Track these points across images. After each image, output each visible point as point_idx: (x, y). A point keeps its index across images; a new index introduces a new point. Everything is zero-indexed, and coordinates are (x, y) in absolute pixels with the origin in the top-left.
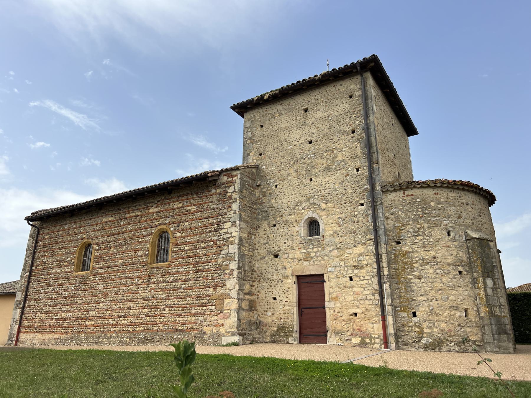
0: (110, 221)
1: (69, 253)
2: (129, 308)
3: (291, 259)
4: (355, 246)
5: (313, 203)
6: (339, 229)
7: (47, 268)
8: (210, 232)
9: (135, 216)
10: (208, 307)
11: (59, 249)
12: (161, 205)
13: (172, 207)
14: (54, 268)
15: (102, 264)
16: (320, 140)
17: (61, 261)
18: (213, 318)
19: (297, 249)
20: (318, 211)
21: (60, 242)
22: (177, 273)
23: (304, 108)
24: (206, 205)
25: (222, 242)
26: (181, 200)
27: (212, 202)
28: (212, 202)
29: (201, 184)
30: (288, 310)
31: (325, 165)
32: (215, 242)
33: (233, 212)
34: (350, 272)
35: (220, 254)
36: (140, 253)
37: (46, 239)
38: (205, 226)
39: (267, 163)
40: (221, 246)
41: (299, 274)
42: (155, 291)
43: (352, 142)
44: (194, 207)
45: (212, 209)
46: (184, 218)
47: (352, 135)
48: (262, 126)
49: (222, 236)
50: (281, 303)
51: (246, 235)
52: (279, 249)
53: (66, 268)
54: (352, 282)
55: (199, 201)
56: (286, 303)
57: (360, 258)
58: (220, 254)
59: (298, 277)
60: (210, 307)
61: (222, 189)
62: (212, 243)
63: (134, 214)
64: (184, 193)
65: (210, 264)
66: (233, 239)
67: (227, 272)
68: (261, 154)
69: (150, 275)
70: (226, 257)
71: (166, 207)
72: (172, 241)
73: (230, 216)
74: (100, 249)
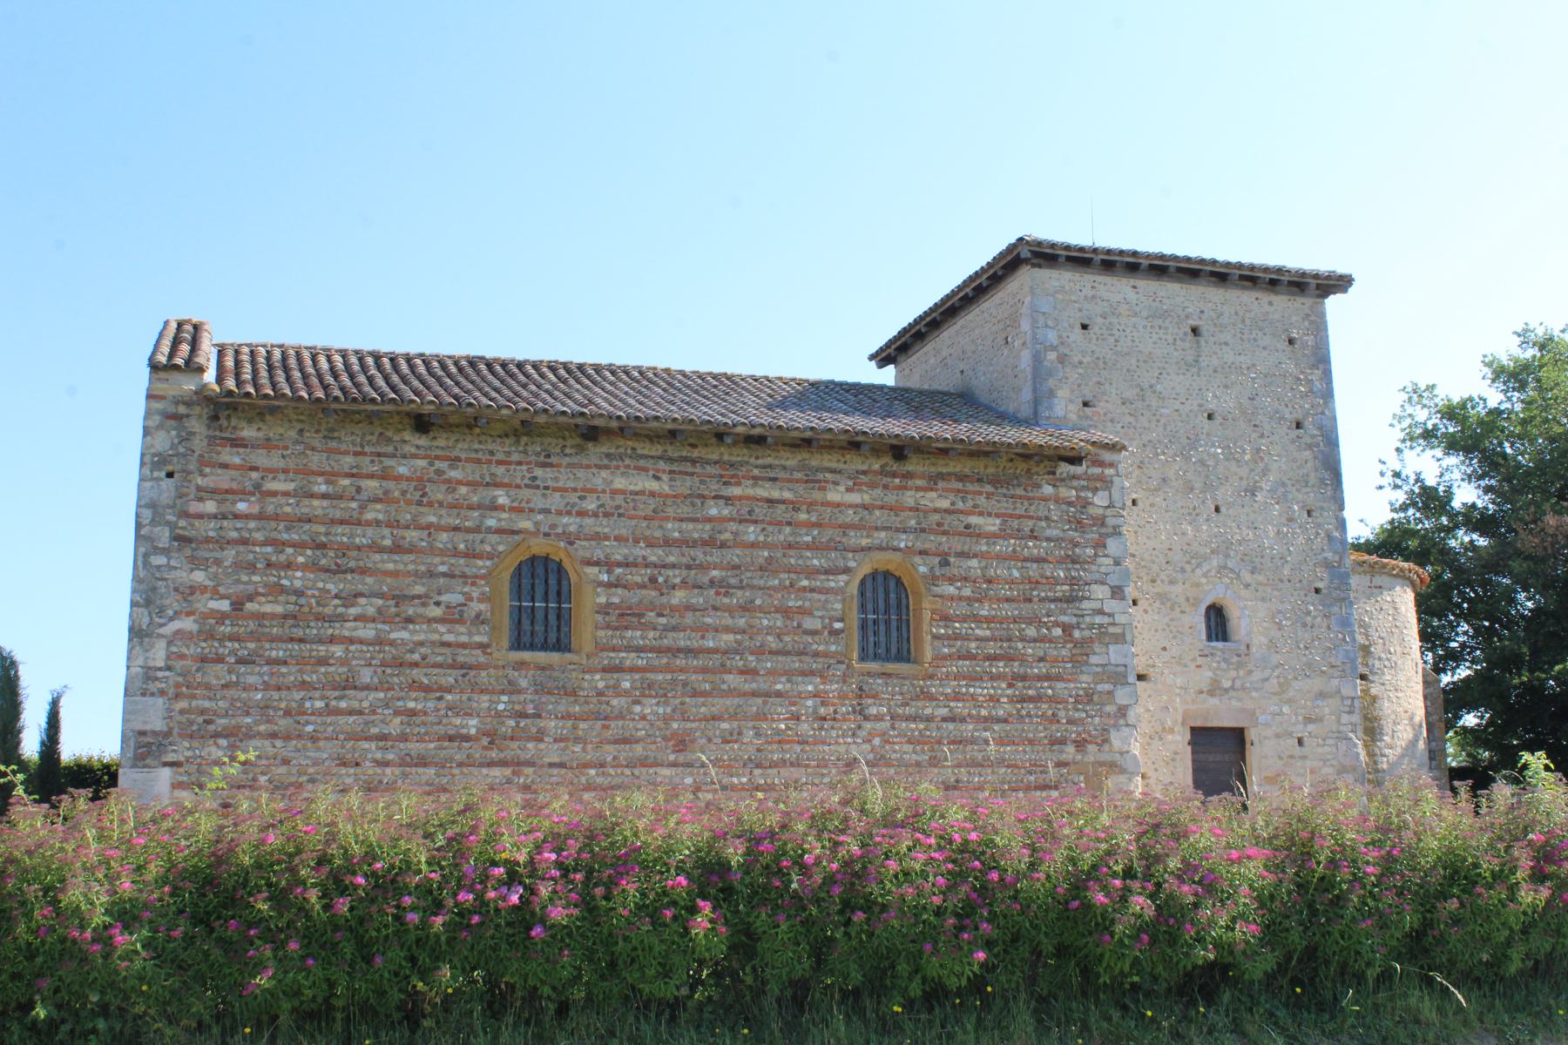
0: (652, 494)
1: (444, 575)
5: (1225, 567)
6: (1279, 634)
7: (320, 617)
9: (771, 502)
11: (376, 548)
12: (872, 486)
13: (911, 502)
17: (400, 599)
19: (1192, 666)
22: (957, 697)
24: (1031, 523)
28: (1047, 518)
31: (1244, 483)
32: (1067, 629)
34: (1301, 727)
36: (809, 623)
41: (1199, 724)
42: (887, 742)
43: (1299, 449)
44: (990, 520)
45: (1048, 539)
48: (1084, 327)
49: (1088, 619)
53: (442, 628)
55: (1005, 506)
57: (1319, 702)
58: (1086, 663)
59: (1193, 729)
62: (1058, 632)
63: (762, 491)
64: (951, 469)
65: (1060, 685)
66: (1118, 630)
67: (1108, 708)
68: (1086, 404)
70: (1104, 672)
71: (891, 498)
72: (927, 605)
73: (1103, 569)
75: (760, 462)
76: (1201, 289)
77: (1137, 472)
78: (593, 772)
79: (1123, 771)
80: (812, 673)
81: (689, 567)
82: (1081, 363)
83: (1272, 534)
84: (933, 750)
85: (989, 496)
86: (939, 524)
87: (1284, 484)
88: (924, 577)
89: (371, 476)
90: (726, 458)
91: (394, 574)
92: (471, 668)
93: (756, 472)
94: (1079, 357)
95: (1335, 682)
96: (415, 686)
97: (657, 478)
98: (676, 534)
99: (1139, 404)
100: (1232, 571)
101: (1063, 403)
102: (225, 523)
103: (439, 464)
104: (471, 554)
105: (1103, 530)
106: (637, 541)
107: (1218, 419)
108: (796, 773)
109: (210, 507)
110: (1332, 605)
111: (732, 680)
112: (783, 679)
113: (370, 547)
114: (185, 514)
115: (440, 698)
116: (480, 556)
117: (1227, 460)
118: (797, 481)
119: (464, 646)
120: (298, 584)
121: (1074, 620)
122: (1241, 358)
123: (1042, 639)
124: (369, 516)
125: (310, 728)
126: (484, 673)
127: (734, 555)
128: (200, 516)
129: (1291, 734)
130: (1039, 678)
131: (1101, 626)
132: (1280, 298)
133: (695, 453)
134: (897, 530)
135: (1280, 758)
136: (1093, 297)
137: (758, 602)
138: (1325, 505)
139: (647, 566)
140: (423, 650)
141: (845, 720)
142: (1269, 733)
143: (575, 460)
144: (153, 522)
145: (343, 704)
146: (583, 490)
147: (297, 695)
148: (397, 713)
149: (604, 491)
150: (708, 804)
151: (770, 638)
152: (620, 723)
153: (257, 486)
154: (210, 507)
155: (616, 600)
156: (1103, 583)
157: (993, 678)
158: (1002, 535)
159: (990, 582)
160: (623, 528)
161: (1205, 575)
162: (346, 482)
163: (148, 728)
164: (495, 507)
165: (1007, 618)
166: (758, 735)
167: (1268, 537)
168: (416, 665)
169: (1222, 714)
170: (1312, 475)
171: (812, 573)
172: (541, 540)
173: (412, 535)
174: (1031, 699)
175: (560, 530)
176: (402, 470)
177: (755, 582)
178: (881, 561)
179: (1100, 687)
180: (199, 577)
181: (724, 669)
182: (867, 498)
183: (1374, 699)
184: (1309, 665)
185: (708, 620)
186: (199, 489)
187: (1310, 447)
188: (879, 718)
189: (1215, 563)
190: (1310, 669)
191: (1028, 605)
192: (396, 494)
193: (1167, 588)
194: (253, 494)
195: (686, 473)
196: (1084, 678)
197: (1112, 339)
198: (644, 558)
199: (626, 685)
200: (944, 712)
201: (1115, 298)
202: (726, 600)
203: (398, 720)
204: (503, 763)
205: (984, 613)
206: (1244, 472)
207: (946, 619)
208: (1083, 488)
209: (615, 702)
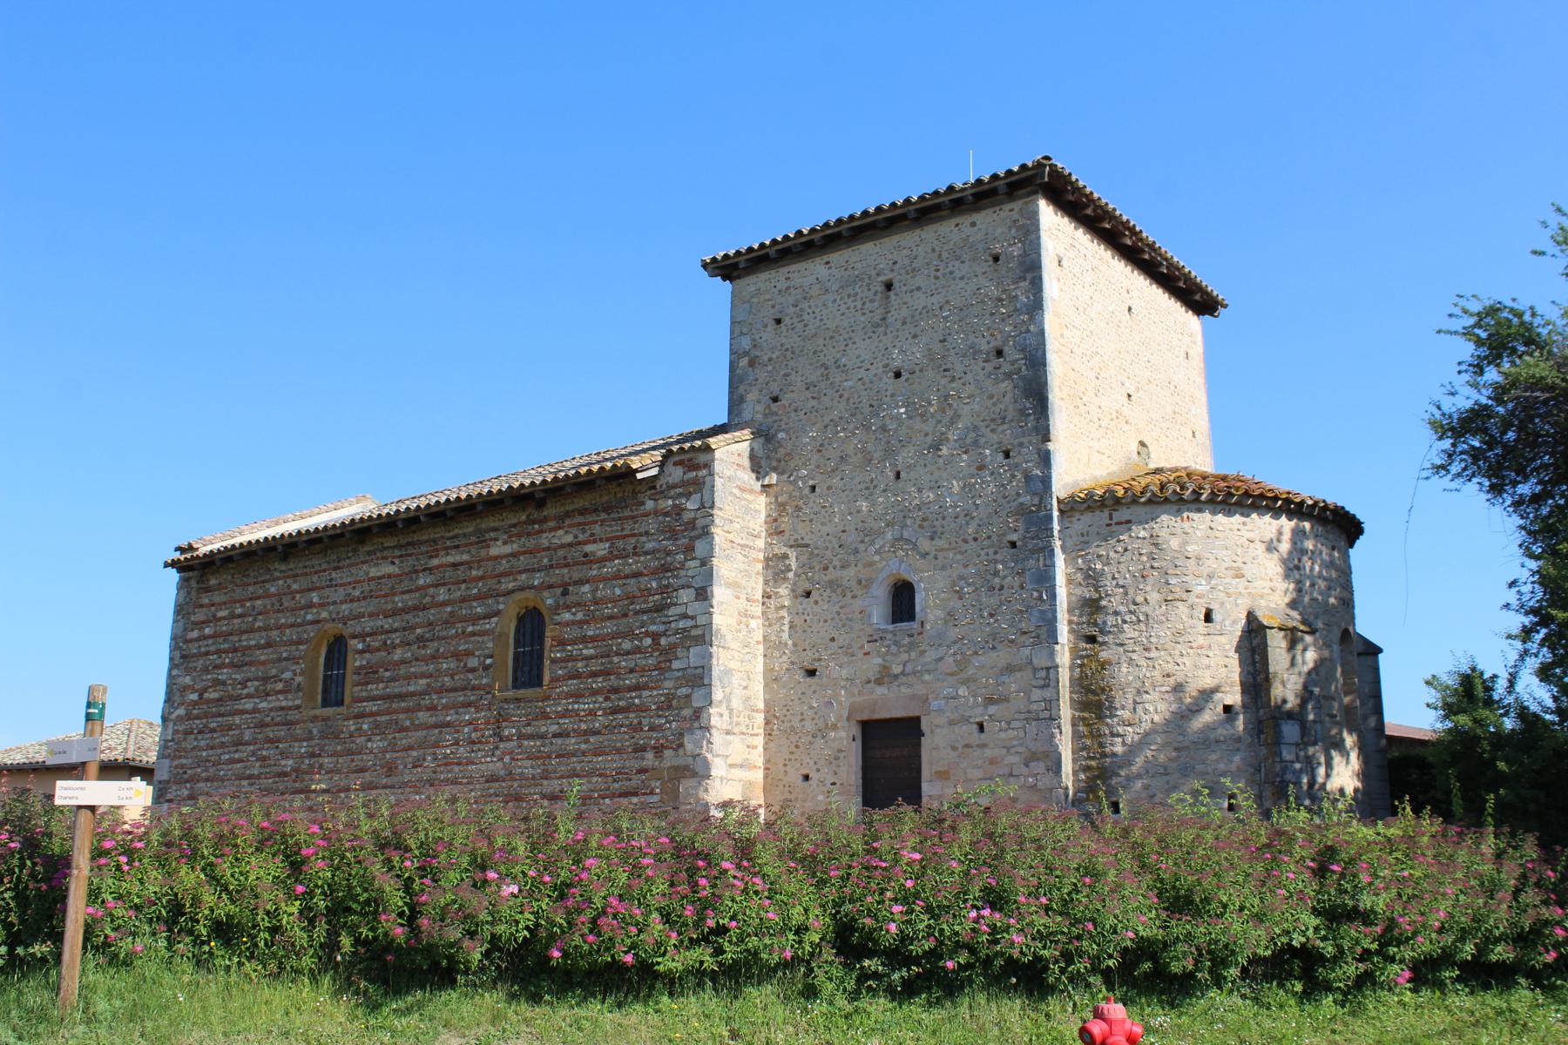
0: (390, 576)
4: (994, 648)
5: (901, 539)
8: (644, 612)
9: (455, 565)
11: (259, 647)
12: (519, 536)
14: (249, 696)
15: (375, 689)
17: (265, 680)
19: (860, 655)
21: (259, 629)
23: (882, 278)
24: (633, 540)
25: (672, 639)
26: (570, 526)
28: (647, 533)
31: (929, 439)
32: (655, 637)
34: (980, 710)
35: (670, 669)
36: (473, 662)
38: (632, 598)
40: (673, 647)
41: (865, 717)
43: (997, 382)
44: (602, 545)
46: (576, 576)
47: (996, 362)
48: (778, 321)
51: (733, 621)
53: (281, 697)
54: (983, 736)
57: (1004, 678)
58: (670, 669)
62: (649, 641)
65: (647, 693)
67: (687, 712)
68: (775, 400)
69: (501, 719)
71: (531, 543)
72: (548, 634)
73: (690, 573)
76: (896, 238)
77: (816, 457)
79: (694, 774)
81: (404, 629)
83: (956, 489)
87: (976, 428)
88: (550, 608)
89: (259, 598)
91: (263, 663)
95: (1026, 651)
99: (822, 385)
100: (908, 541)
104: (299, 643)
105: (693, 534)
107: (905, 375)
110: (1027, 559)
111: (423, 716)
114: (187, 641)
119: (289, 708)
121: (662, 628)
122: (933, 299)
123: (637, 650)
128: (191, 641)
129: (966, 720)
131: (684, 629)
132: (984, 213)
134: (534, 570)
135: (954, 748)
138: (1025, 440)
142: (942, 720)
154: (195, 634)
157: (595, 693)
158: (610, 557)
159: (596, 603)
161: (877, 552)
164: (311, 605)
167: (951, 495)
168: (267, 725)
169: (891, 704)
170: (1011, 408)
176: (273, 590)
180: (188, 680)
181: (418, 708)
183: (1104, 665)
184: (994, 635)
187: (1009, 376)
188: (509, 739)
189: (889, 536)
190: (994, 641)
191: (625, 620)
193: (839, 573)
196: (668, 684)
197: (800, 326)
200: (554, 728)
205: (590, 633)
206: (928, 427)
207: (562, 643)
208: (680, 495)
209: (358, 741)
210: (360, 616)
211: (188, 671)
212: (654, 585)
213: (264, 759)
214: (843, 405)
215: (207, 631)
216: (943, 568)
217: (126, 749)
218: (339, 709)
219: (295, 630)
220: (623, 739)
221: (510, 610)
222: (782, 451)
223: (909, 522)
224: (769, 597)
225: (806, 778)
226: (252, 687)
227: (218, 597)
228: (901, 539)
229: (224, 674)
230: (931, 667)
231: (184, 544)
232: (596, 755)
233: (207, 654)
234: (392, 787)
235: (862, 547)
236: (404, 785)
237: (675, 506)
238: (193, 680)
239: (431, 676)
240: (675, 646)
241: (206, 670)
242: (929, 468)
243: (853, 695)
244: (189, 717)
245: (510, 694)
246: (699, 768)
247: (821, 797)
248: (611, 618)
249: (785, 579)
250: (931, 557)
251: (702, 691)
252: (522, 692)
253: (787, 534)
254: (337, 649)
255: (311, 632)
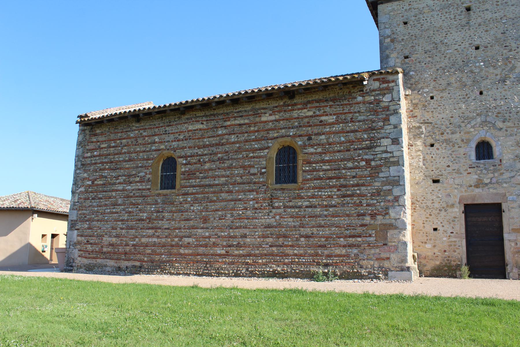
0: (200, 130)
1: (140, 167)
2: (245, 236)
3: (458, 185)
5: (486, 121)
7: (110, 184)
8: (360, 149)
9: (240, 125)
10: (364, 239)
11: (125, 161)
12: (279, 112)
13: (296, 116)
14: (119, 183)
16: (491, 46)
17: (129, 176)
18: (373, 251)
19: (465, 173)
20: (493, 131)
21: (125, 153)
22: (313, 197)
23: (465, 5)
24: (351, 115)
26: (310, 108)
27: (359, 112)
28: (359, 112)
29: (341, 89)
30: (455, 242)
31: (498, 77)
32: (368, 161)
33: (392, 127)
35: (378, 177)
36: (253, 171)
37: (102, 148)
38: (352, 142)
39: (417, 69)
42: (282, 217)
44: (331, 117)
45: (359, 121)
46: (316, 131)
48: (405, 23)
49: (379, 156)
50: (445, 234)
52: (440, 173)
53: (139, 184)
55: (339, 110)
56: (452, 235)
58: (378, 177)
60: (368, 239)
61: (373, 98)
62: (364, 163)
64: (314, 98)
65: (363, 188)
66: (395, 159)
67: (389, 198)
68: (406, 57)
69: (272, 198)
70: (387, 181)
71: (287, 115)
72: (300, 158)
73: (388, 131)
74: (188, 163)
75: (237, 110)
77: (434, 83)
78: (177, 231)
79: (396, 228)
80: (253, 191)
81: (211, 154)
82: (403, 40)
84: (301, 220)
85: (331, 106)
86: (308, 123)
88: (301, 146)
89: (124, 139)
90: (225, 111)
91: (128, 168)
92: (146, 196)
93: (235, 115)
94: (402, 37)
96: (132, 204)
97: (202, 124)
98: (207, 143)
99: (434, 51)
101: (393, 60)
102: (92, 159)
103: (141, 131)
104: (148, 159)
105: (388, 113)
106: (195, 147)
107: (481, 49)
108: (247, 231)
109: (89, 155)
111: (224, 195)
112: (242, 194)
113: (123, 161)
114: (84, 158)
115: (137, 207)
116: (150, 160)
117: (487, 67)
118: (250, 115)
119: (144, 189)
120: (106, 174)
121: (372, 157)
124: (123, 151)
125: (106, 218)
126: (149, 198)
127: (227, 148)
128: (87, 158)
130: (353, 186)
131: (386, 158)
133: (215, 112)
134: (289, 128)
136: (410, 9)
137: (234, 164)
139: (197, 156)
140: (133, 192)
141: (265, 209)
143: (178, 122)
144: (78, 161)
145: (114, 210)
146: (180, 132)
147: (104, 208)
148: (126, 213)
149: (185, 132)
150: (214, 243)
151: (238, 178)
152: (186, 213)
153: (99, 147)
154: (89, 155)
155: (187, 169)
156: (387, 138)
158: (337, 122)
160: (191, 143)
161: (473, 127)
162: (118, 142)
163: (73, 219)
164: (155, 143)
165: (338, 159)
166: (232, 216)
167: (514, 102)
168: (131, 197)
169: (484, 196)
171: (254, 150)
172: (166, 151)
173: (133, 155)
174: (349, 196)
175: (172, 147)
176: (132, 135)
177: (233, 157)
178: (287, 141)
179: (384, 188)
180: (85, 175)
181: (221, 192)
182: (277, 117)
185: (217, 173)
186: (87, 150)
188: (279, 208)
189: (479, 120)
192: (130, 143)
193: (450, 136)
194: (98, 149)
195: (212, 120)
196: (376, 184)
198: (197, 153)
199: (189, 199)
200: (307, 203)
201: (421, 6)
202: (223, 165)
203: (126, 215)
204: (152, 228)
205: (327, 158)
207: (309, 163)
209: (185, 206)
210: (183, 148)
211: (85, 171)
212: (366, 136)
213: (130, 212)
214: (446, 61)
215: (95, 153)
216: (511, 135)
217: (30, 203)
218: (173, 191)
219: (145, 154)
220: (347, 210)
221: (275, 147)
222: (413, 81)
223: (490, 114)
224: (412, 146)
225: (435, 229)
226: (121, 179)
227: (101, 138)
228: (486, 121)
229: (106, 173)
230: (507, 180)
231: (83, 114)
232: (333, 216)
233: (95, 164)
234: (207, 228)
235: (463, 125)
236: (214, 228)
237: (375, 100)
238: (89, 175)
239: (228, 177)
240: (381, 166)
241: (96, 171)
242: (500, 90)
243: (462, 192)
244: (86, 192)
245: (278, 186)
246: (399, 224)
247: (445, 239)
248: (339, 151)
249: (420, 137)
250: (504, 130)
251: (399, 188)
252: (284, 186)
253: (419, 118)
254: (170, 164)
255: (155, 155)
